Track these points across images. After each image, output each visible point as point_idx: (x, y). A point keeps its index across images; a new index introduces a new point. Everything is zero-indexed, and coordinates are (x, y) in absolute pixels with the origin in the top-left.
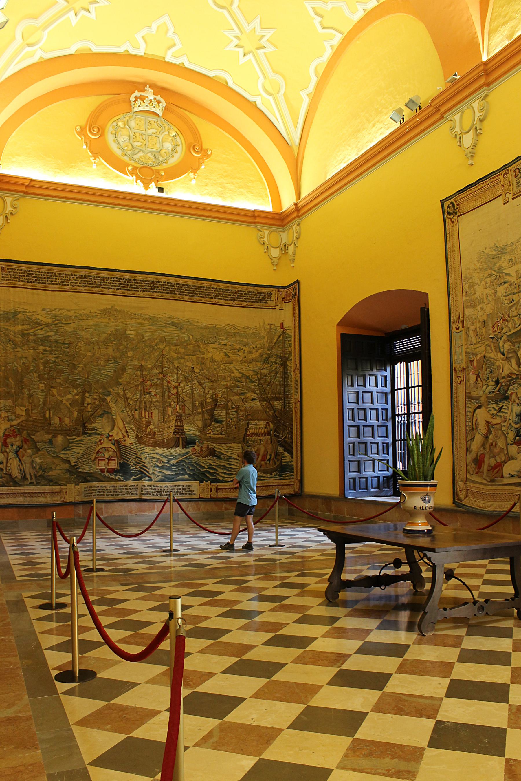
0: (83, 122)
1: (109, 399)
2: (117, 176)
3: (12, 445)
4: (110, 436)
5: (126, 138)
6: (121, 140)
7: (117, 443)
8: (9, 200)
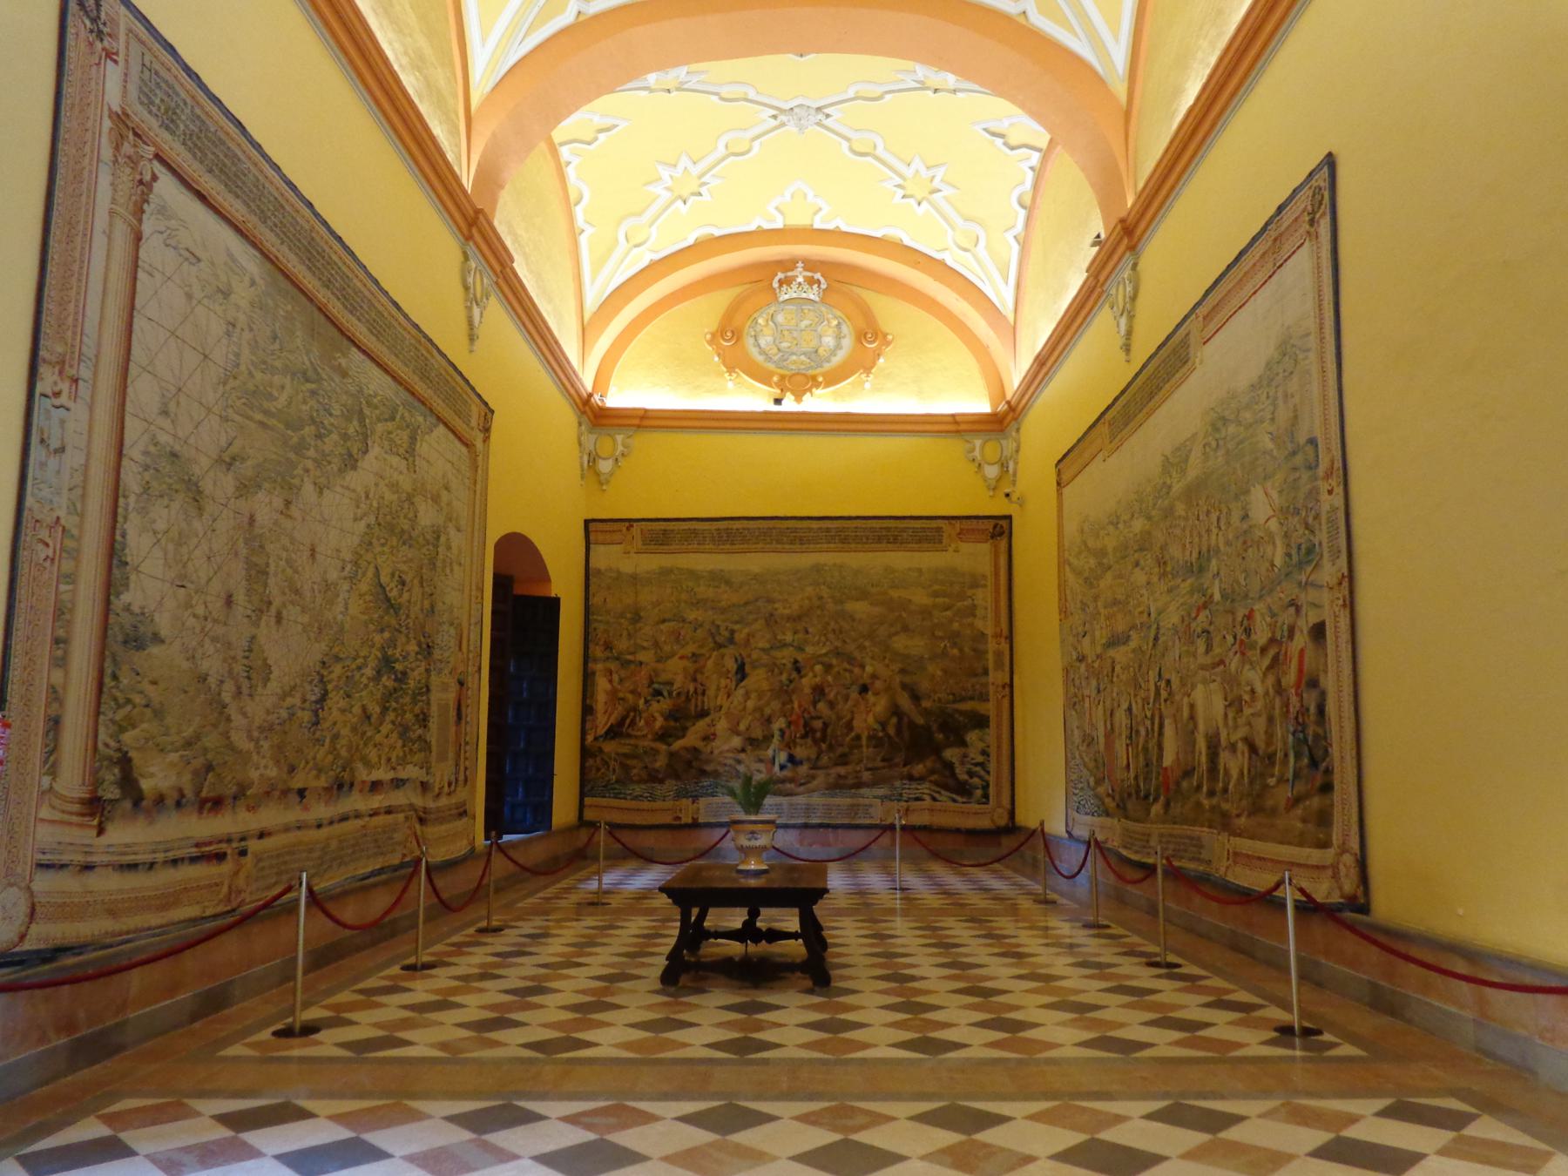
0: (714, 327)
5: (770, 339)
8: (619, 438)
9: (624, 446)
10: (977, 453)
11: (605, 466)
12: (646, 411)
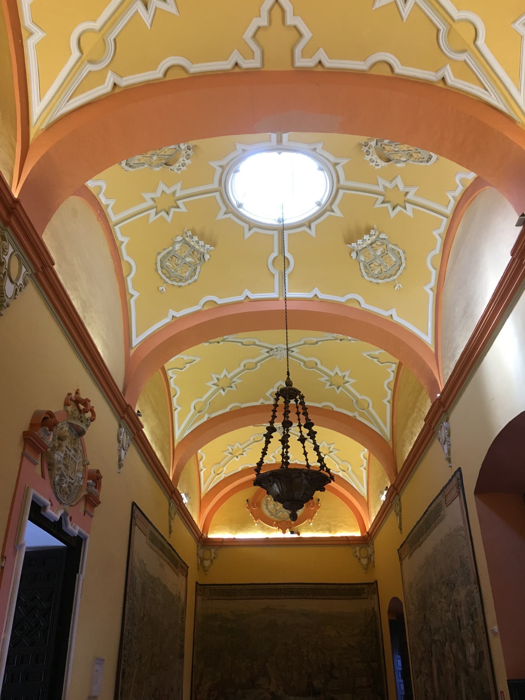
1: (267, 665)
2: (269, 528)
3: (213, 696)
4: (268, 689)
5: (272, 506)
6: (269, 507)
7: (272, 694)
8: (213, 551)
9: (215, 554)
10: (358, 553)
11: (207, 563)
12: (223, 539)
